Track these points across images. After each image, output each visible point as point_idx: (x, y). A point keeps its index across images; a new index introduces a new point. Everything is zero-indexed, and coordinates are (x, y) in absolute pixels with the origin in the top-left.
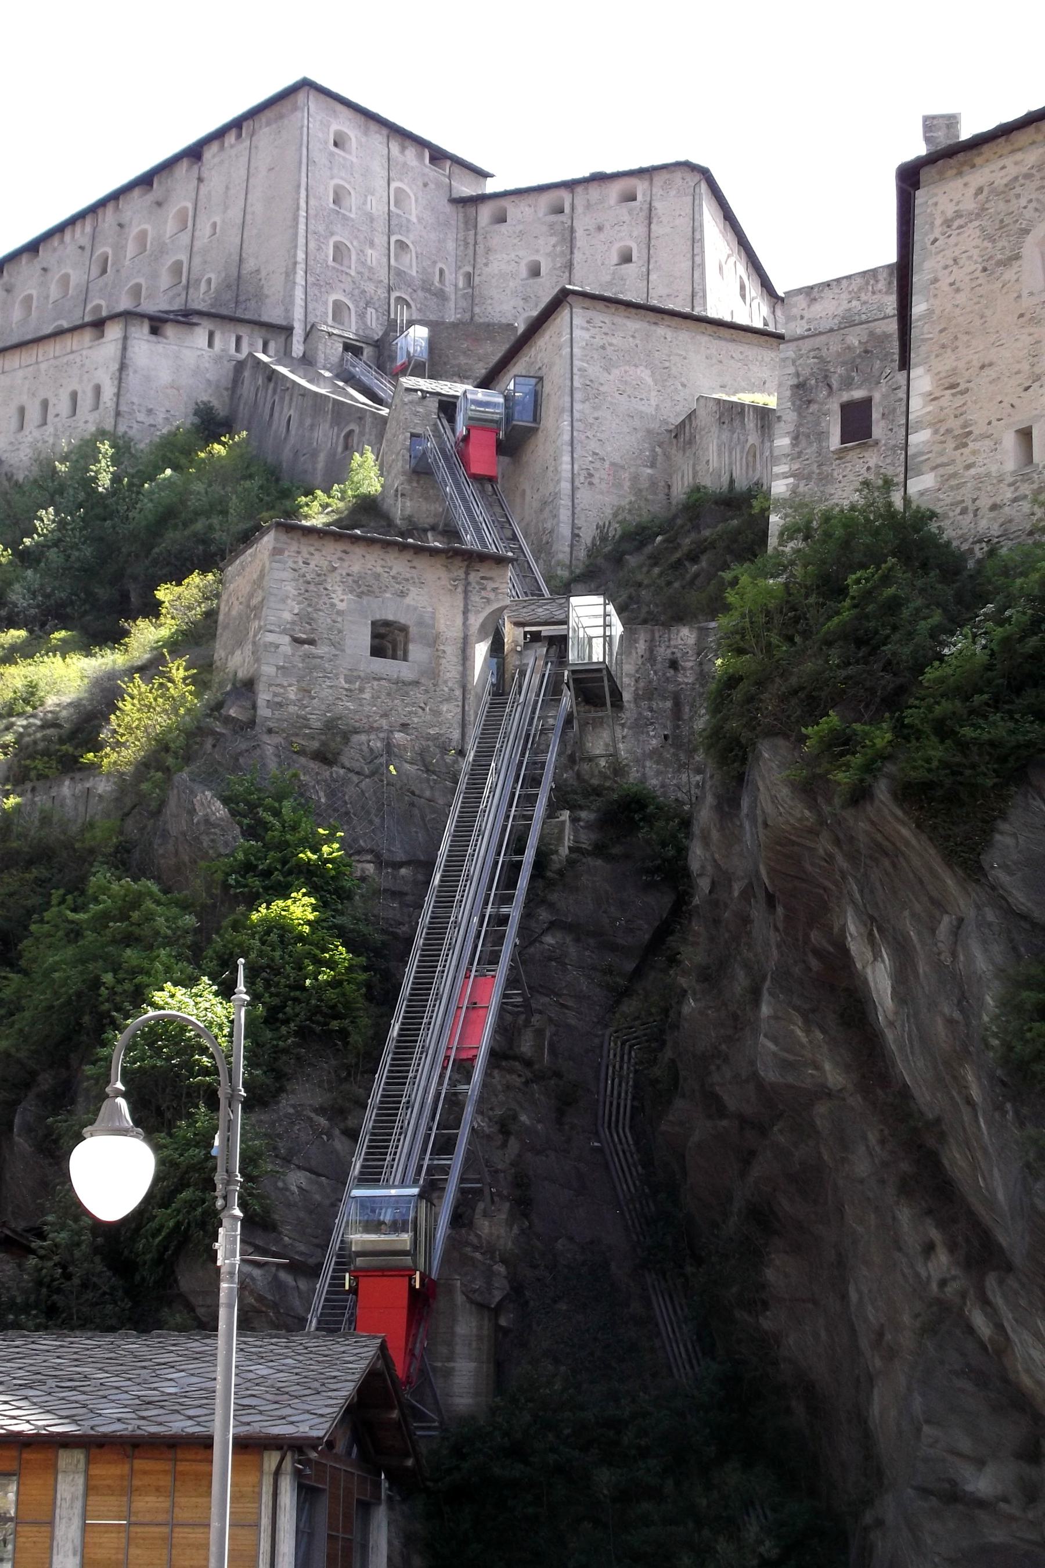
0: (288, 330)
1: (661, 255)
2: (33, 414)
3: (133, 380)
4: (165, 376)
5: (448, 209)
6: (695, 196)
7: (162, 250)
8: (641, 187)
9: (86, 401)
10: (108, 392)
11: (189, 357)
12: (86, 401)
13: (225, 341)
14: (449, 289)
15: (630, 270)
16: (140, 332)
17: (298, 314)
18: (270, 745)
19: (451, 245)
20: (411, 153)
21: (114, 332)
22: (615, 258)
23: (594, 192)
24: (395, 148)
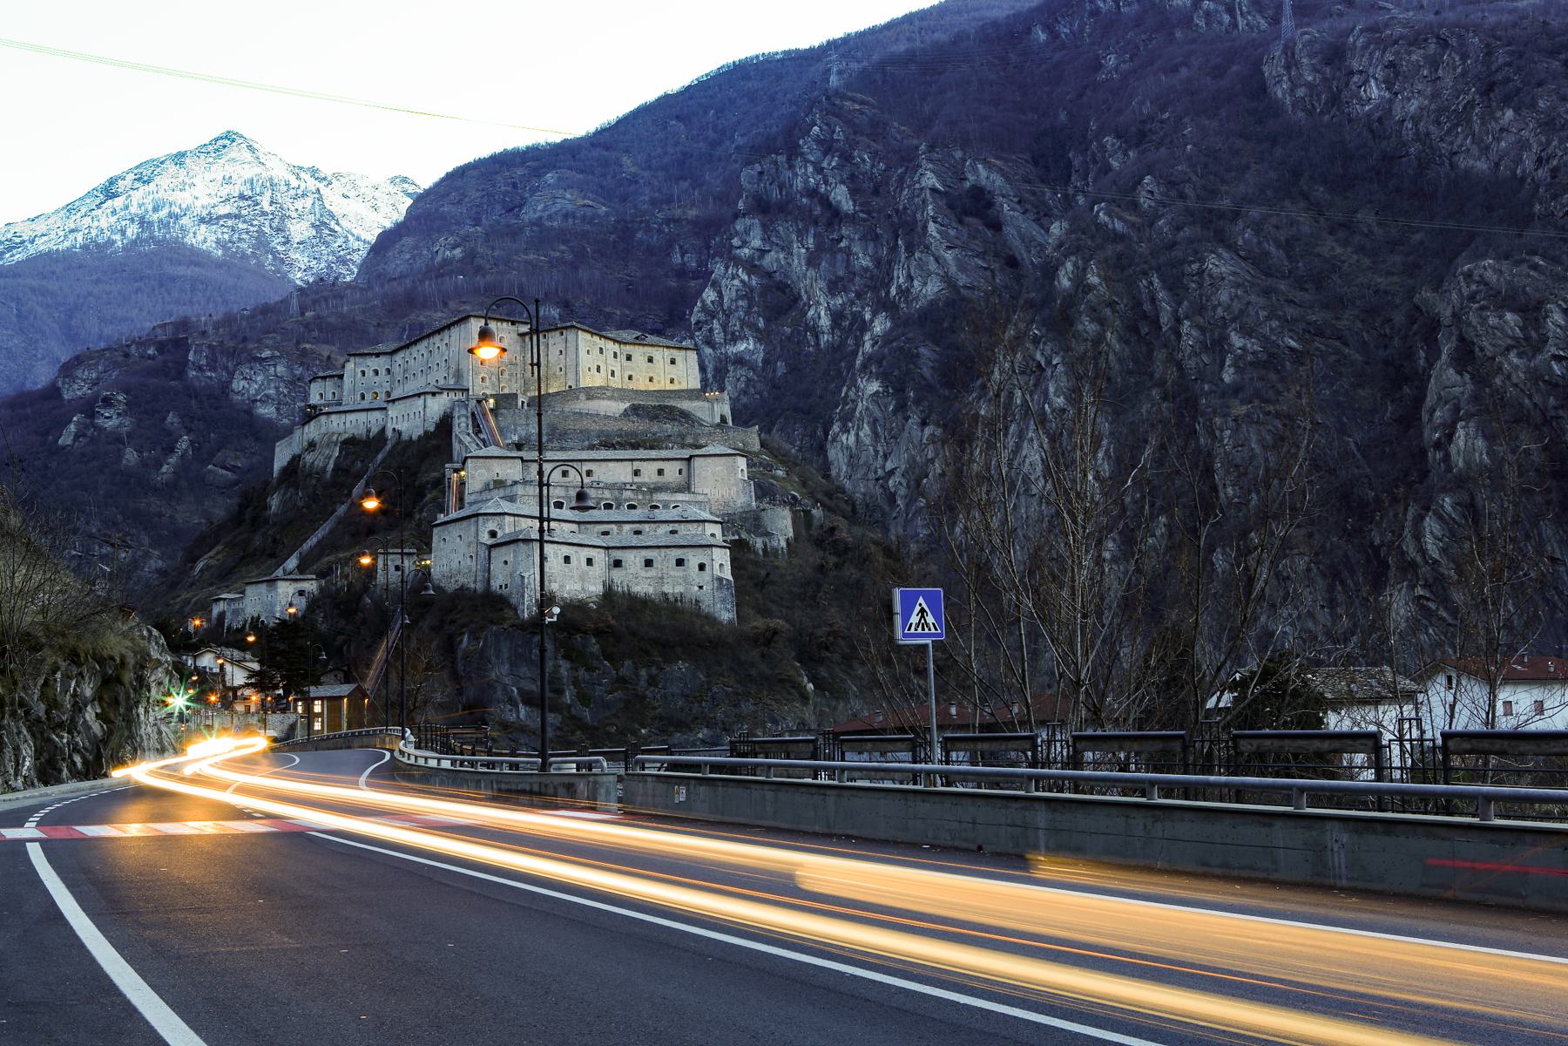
0: (468, 390)
1: (569, 353)
2: (406, 417)
3: (428, 410)
4: (436, 408)
5: (515, 336)
6: (577, 336)
7: (443, 355)
8: (564, 332)
9: (417, 414)
10: (422, 414)
11: (442, 401)
12: (417, 414)
13: (452, 394)
14: (518, 361)
15: (562, 357)
16: (429, 397)
17: (471, 384)
18: (378, 589)
19: (518, 349)
20: (505, 324)
21: (422, 397)
22: (558, 353)
23: (553, 334)
24: (499, 324)
